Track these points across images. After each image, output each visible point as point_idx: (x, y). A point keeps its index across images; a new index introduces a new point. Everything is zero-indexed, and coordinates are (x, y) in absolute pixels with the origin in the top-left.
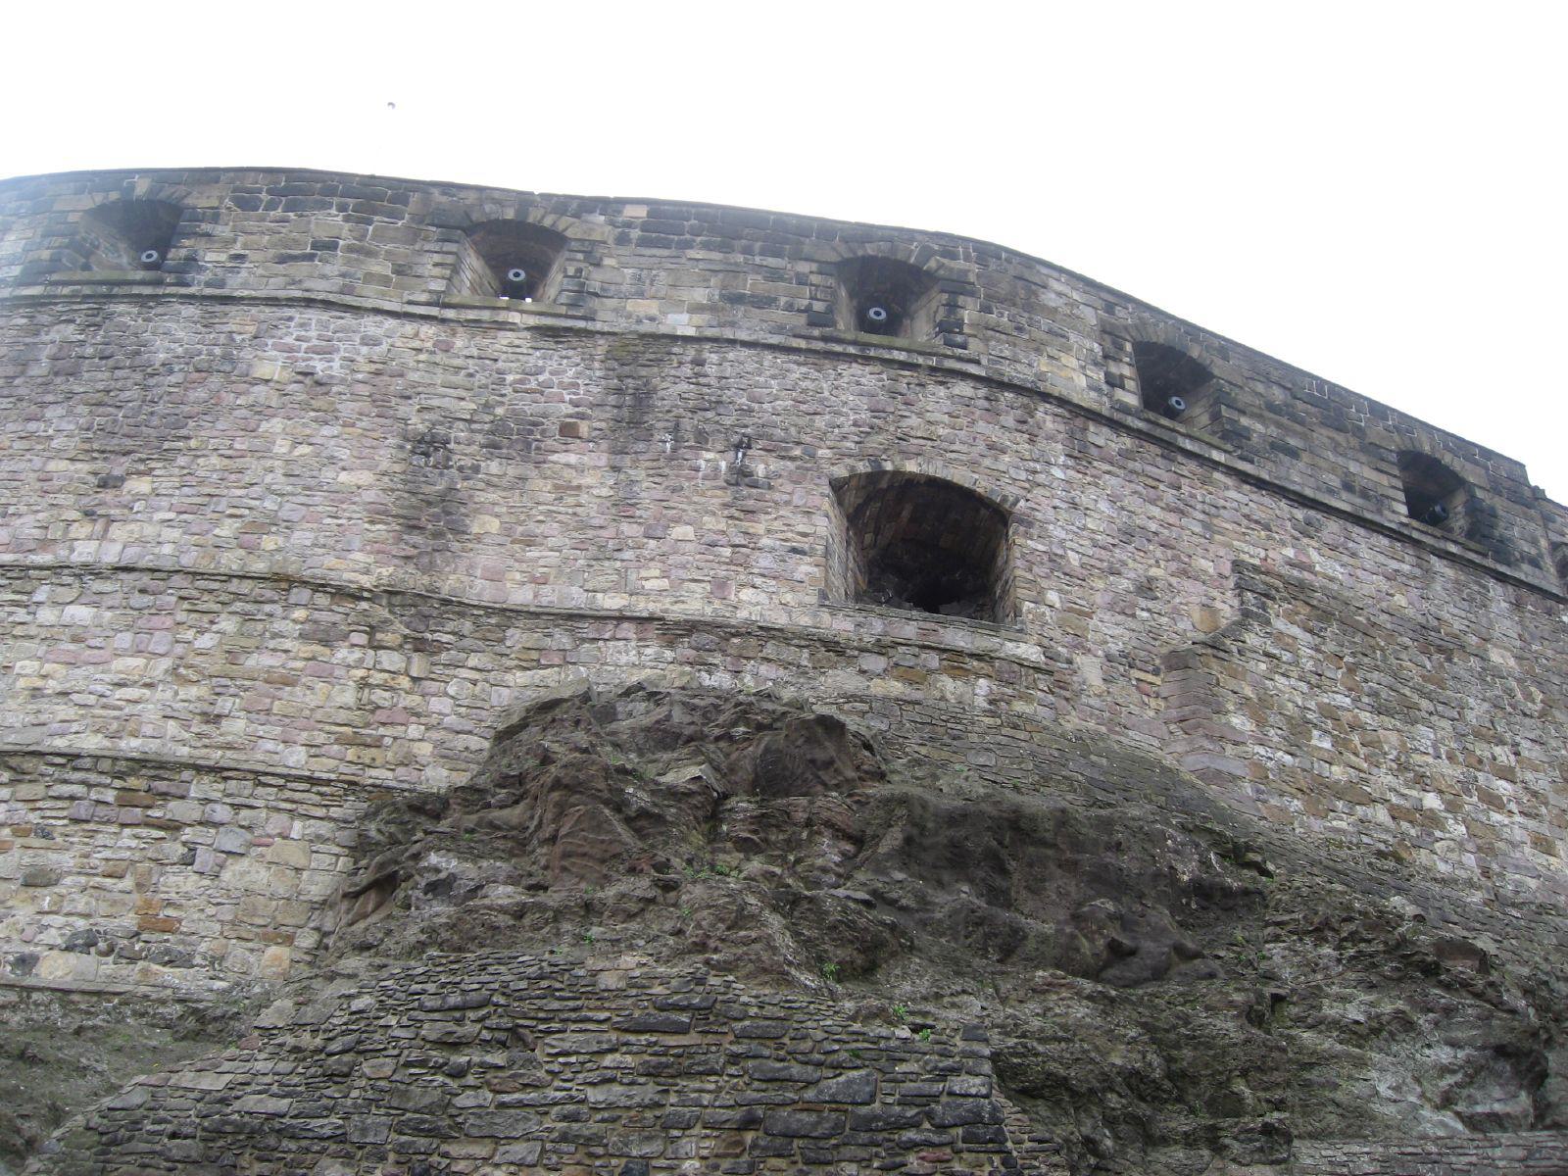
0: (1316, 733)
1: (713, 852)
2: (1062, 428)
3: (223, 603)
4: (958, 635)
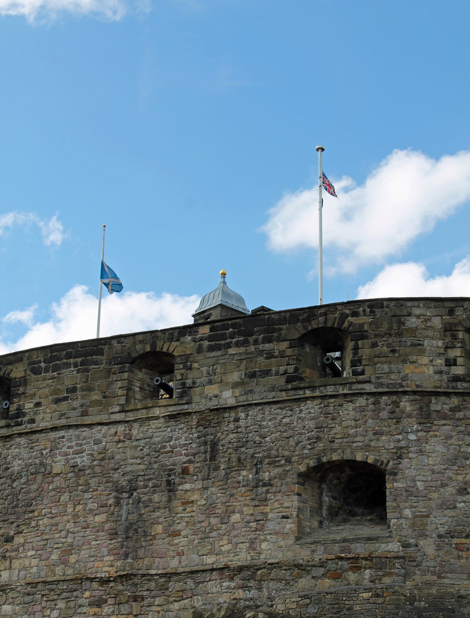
3: (58, 595)
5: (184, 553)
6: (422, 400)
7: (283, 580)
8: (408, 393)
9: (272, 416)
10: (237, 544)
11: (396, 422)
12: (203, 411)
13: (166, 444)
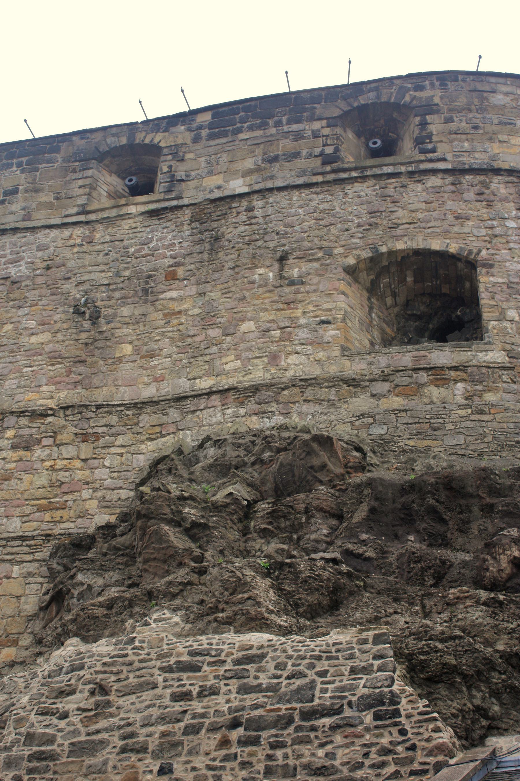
2: (512, 190)
4: (443, 355)
7: (323, 400)
8: (502, 173)
9: (303, 202)
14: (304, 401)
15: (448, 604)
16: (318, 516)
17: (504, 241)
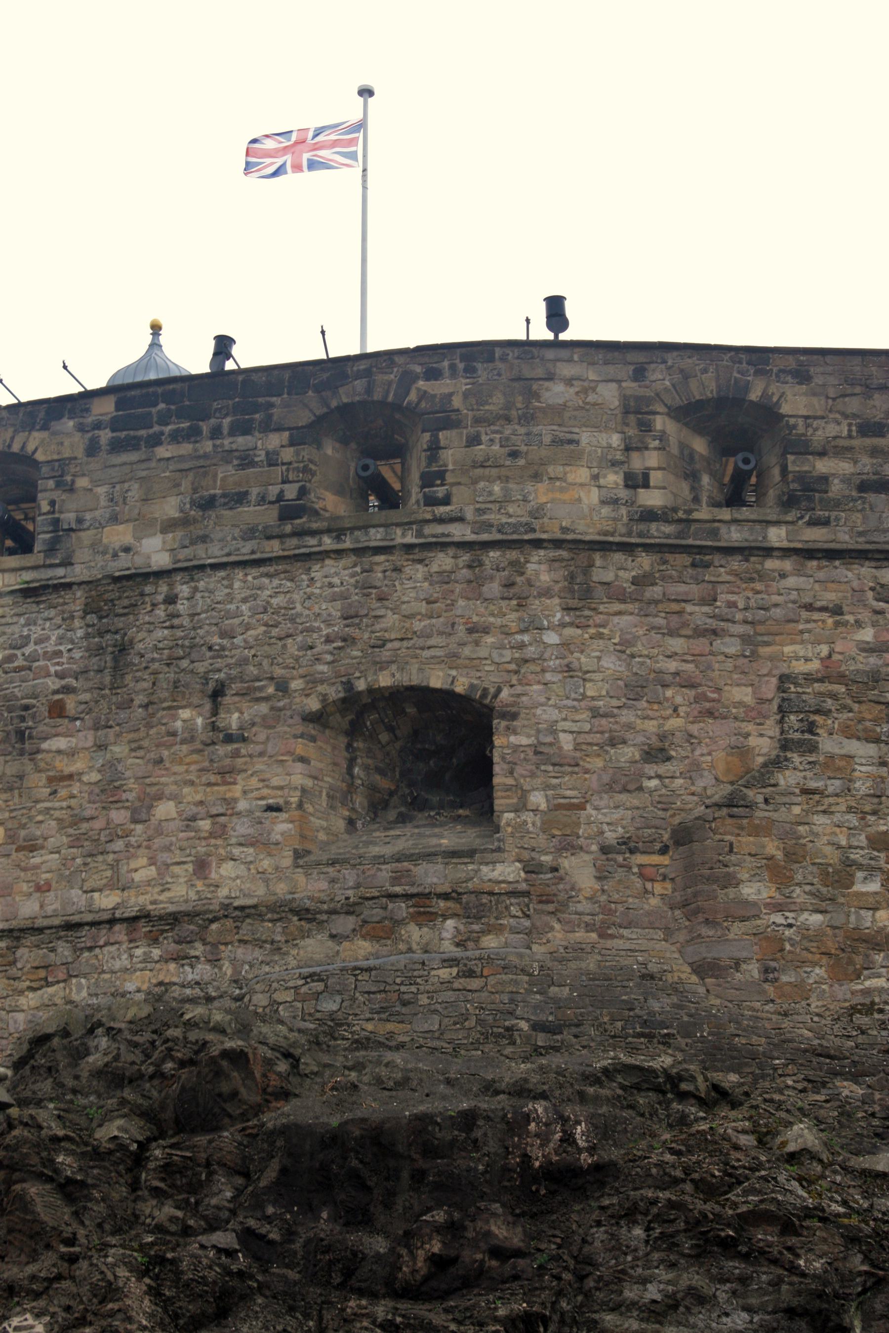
0: (860, 875)
1: (134, 1201)
5: (50, 886)
6: (573, 559)
7: (265, 942)
8: (545, 545)
9: (249, 593)
10: (168, 866)
11: (519, 605)
12: (99, 580)
13: (16, 652)
14: (240, 941)
15: (345, 1320)
16: (220, 1172)
17: (538, 669)
